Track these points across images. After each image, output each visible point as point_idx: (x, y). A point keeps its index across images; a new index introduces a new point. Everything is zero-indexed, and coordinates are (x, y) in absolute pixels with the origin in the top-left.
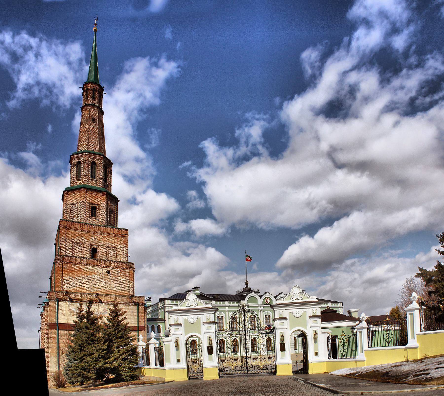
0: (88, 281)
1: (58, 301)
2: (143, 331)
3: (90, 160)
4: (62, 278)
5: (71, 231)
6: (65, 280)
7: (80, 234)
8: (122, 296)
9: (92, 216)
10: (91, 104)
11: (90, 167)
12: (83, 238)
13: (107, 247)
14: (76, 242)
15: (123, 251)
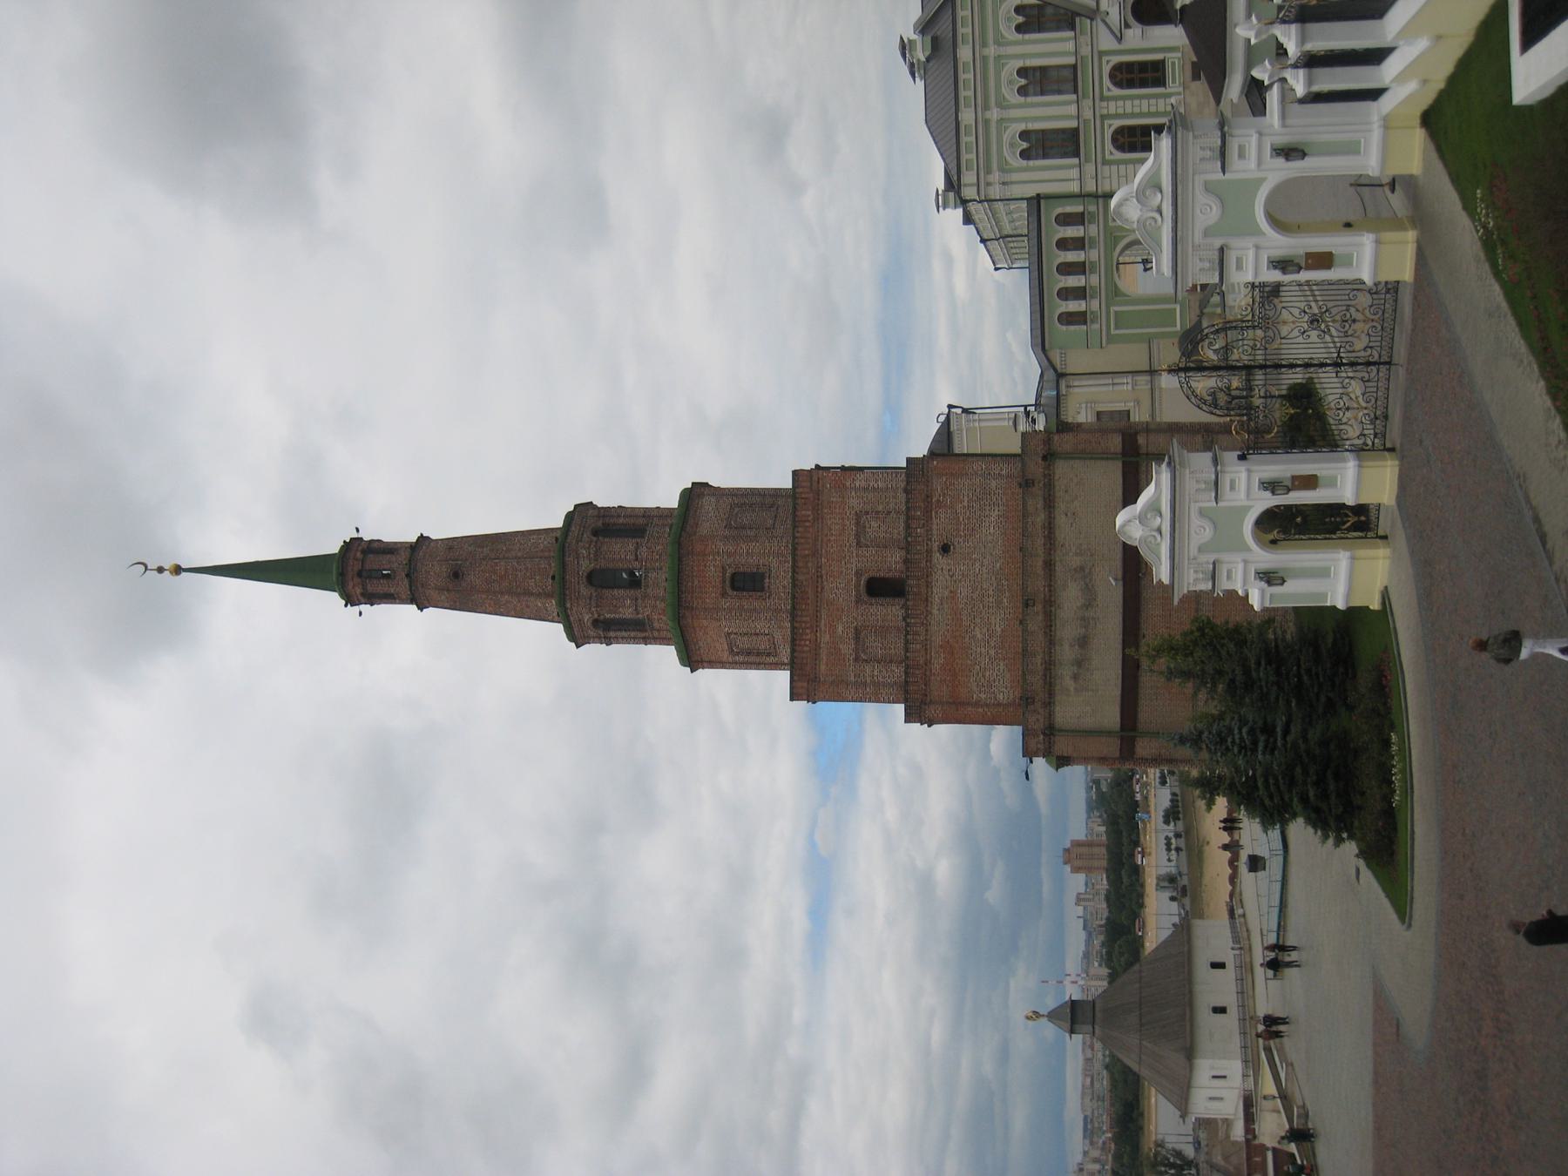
1: (1050, 731)
2: (1141, 440)
4: (977, 704)
5: (823, 667)
8: (1025, 515)
9: (762, 590)
10: (406, 582)
11: (607, 592)
12: (840, 629)
13: (858, 544)
14: (856, 650)
15: (866, 489)
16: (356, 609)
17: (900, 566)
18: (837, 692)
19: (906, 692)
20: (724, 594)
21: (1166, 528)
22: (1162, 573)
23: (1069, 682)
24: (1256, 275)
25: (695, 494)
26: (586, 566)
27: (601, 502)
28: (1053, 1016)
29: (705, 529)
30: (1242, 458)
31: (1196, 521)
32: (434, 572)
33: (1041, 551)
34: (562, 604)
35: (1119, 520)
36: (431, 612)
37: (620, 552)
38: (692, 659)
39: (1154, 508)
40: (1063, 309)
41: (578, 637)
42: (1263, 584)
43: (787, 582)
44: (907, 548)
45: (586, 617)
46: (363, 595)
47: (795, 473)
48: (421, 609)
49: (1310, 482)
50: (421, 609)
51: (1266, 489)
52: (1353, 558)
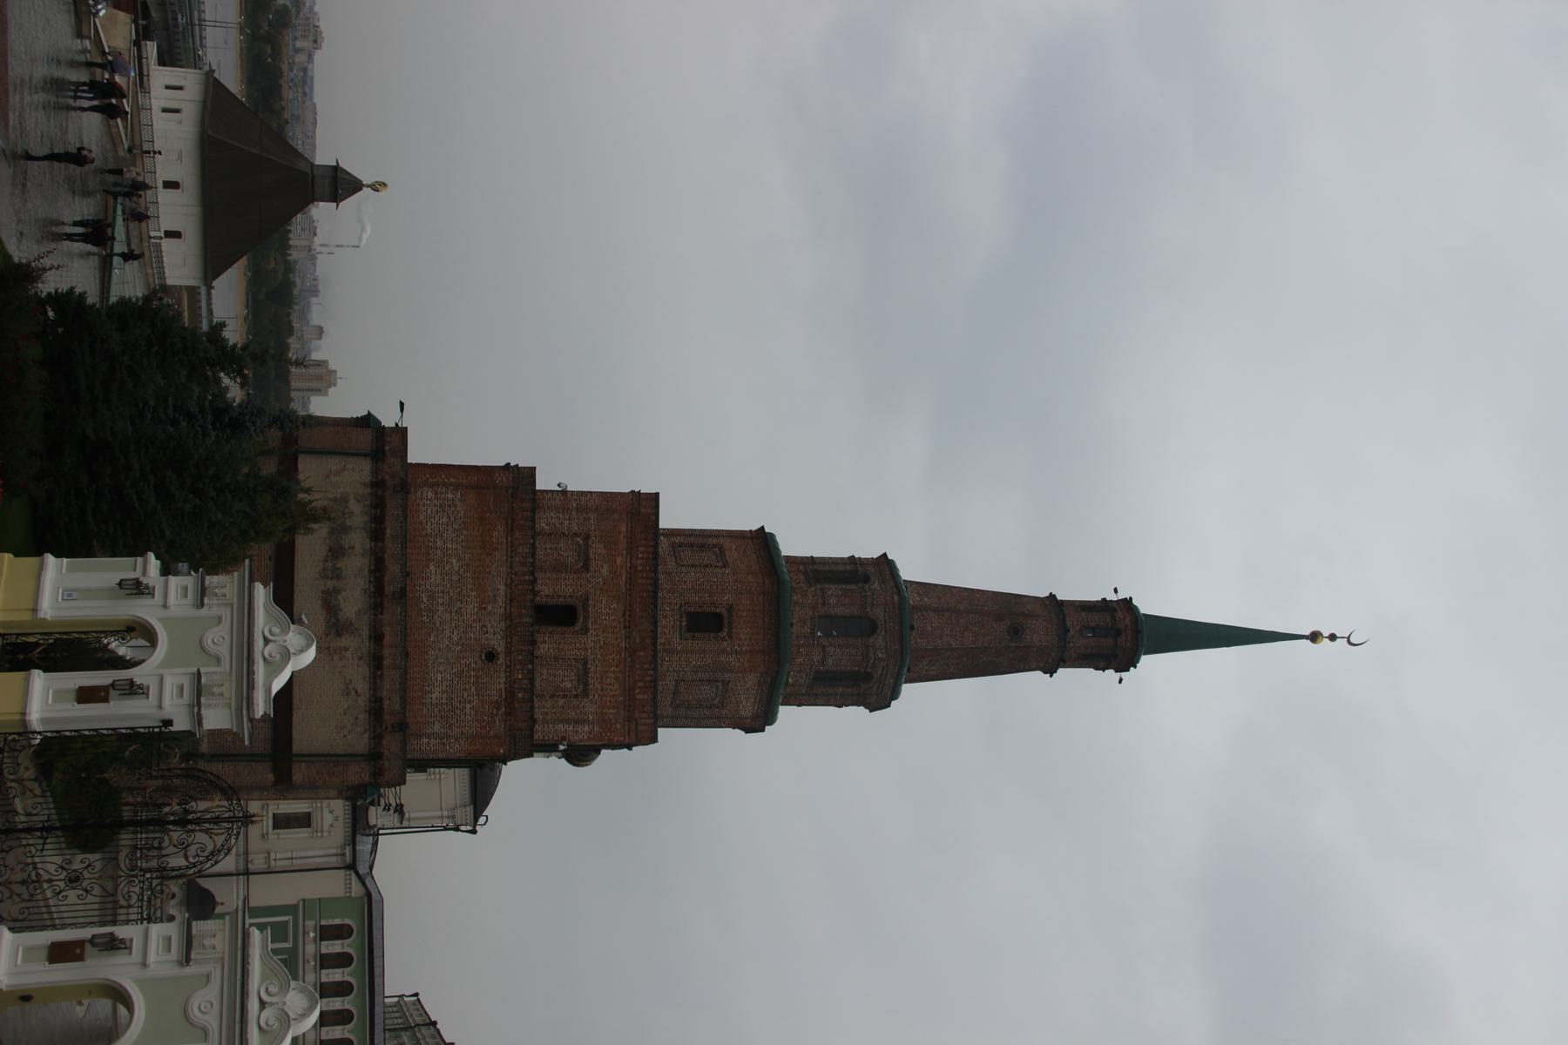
0: (455, 578)
2: (271, 777)
3: (879, 613)
4: (457, 487)
6: (450, 496)
7: (619, 561)
9: (689, 614)
10: (1069, 623)
12: (605, 571)
13: (586, 663)
14: (587, 547)
15: (577, 722)
16: (1121, 596)
17: (539, 637)
18: (607, 503)
19: (534, 501)
20: (730, 609)
21: (259, 642)
22: (261, 593)
23: (356, 508)
24: (147, 931)
25: (758, 721)
26: (879, 640)
27: (861, 711)
28: (355, 186)
29: (751, 680)
30: (168, 723)
31: (224, 651)
32: (1039, 634)
33: (386, 652)
34: (902, 599)
35: (311, 654)
36: (1043, 593)
37: (840, 656)
38: (762, 541)
39: (274, 668)
40: (347, 942)
41: (885, 565)
42: (144, 581)
43: (662, 622)
44: (532, 657)
45: (876, 585)
46: (1115, 610)
47: (654, 740)
48: (1052, 596)
49: (87, 695)
50: (1052, 596)
51: (140, 687)
52: (35, 611)
